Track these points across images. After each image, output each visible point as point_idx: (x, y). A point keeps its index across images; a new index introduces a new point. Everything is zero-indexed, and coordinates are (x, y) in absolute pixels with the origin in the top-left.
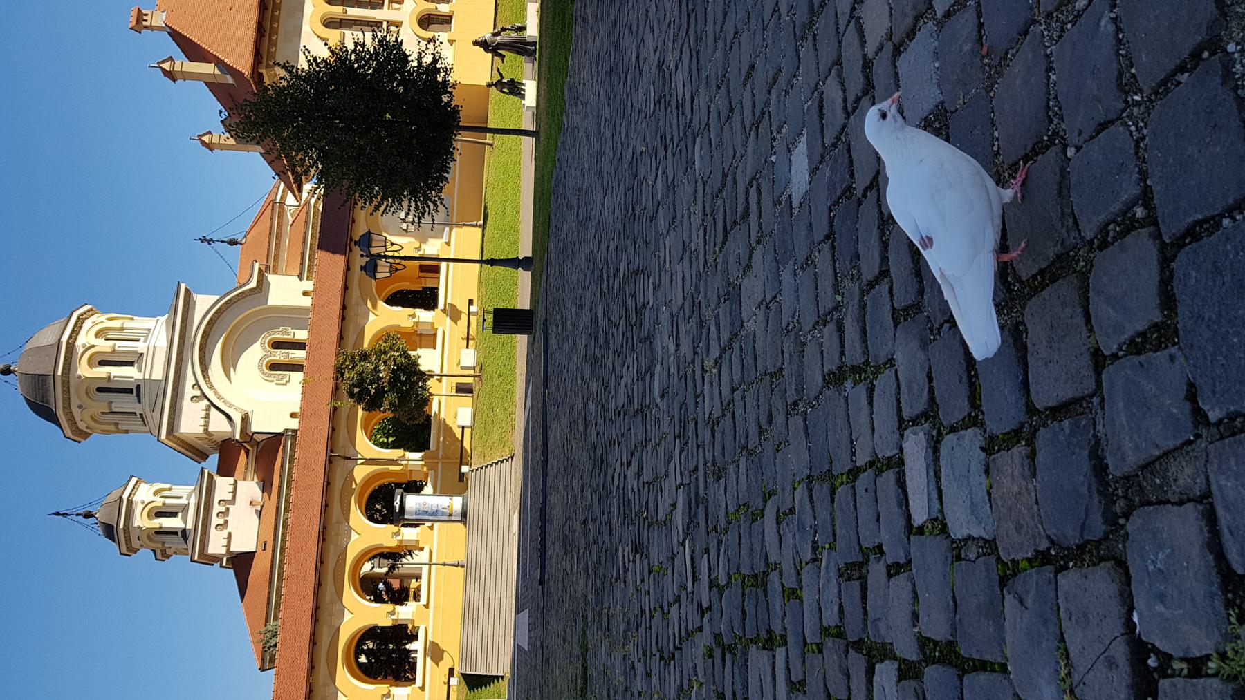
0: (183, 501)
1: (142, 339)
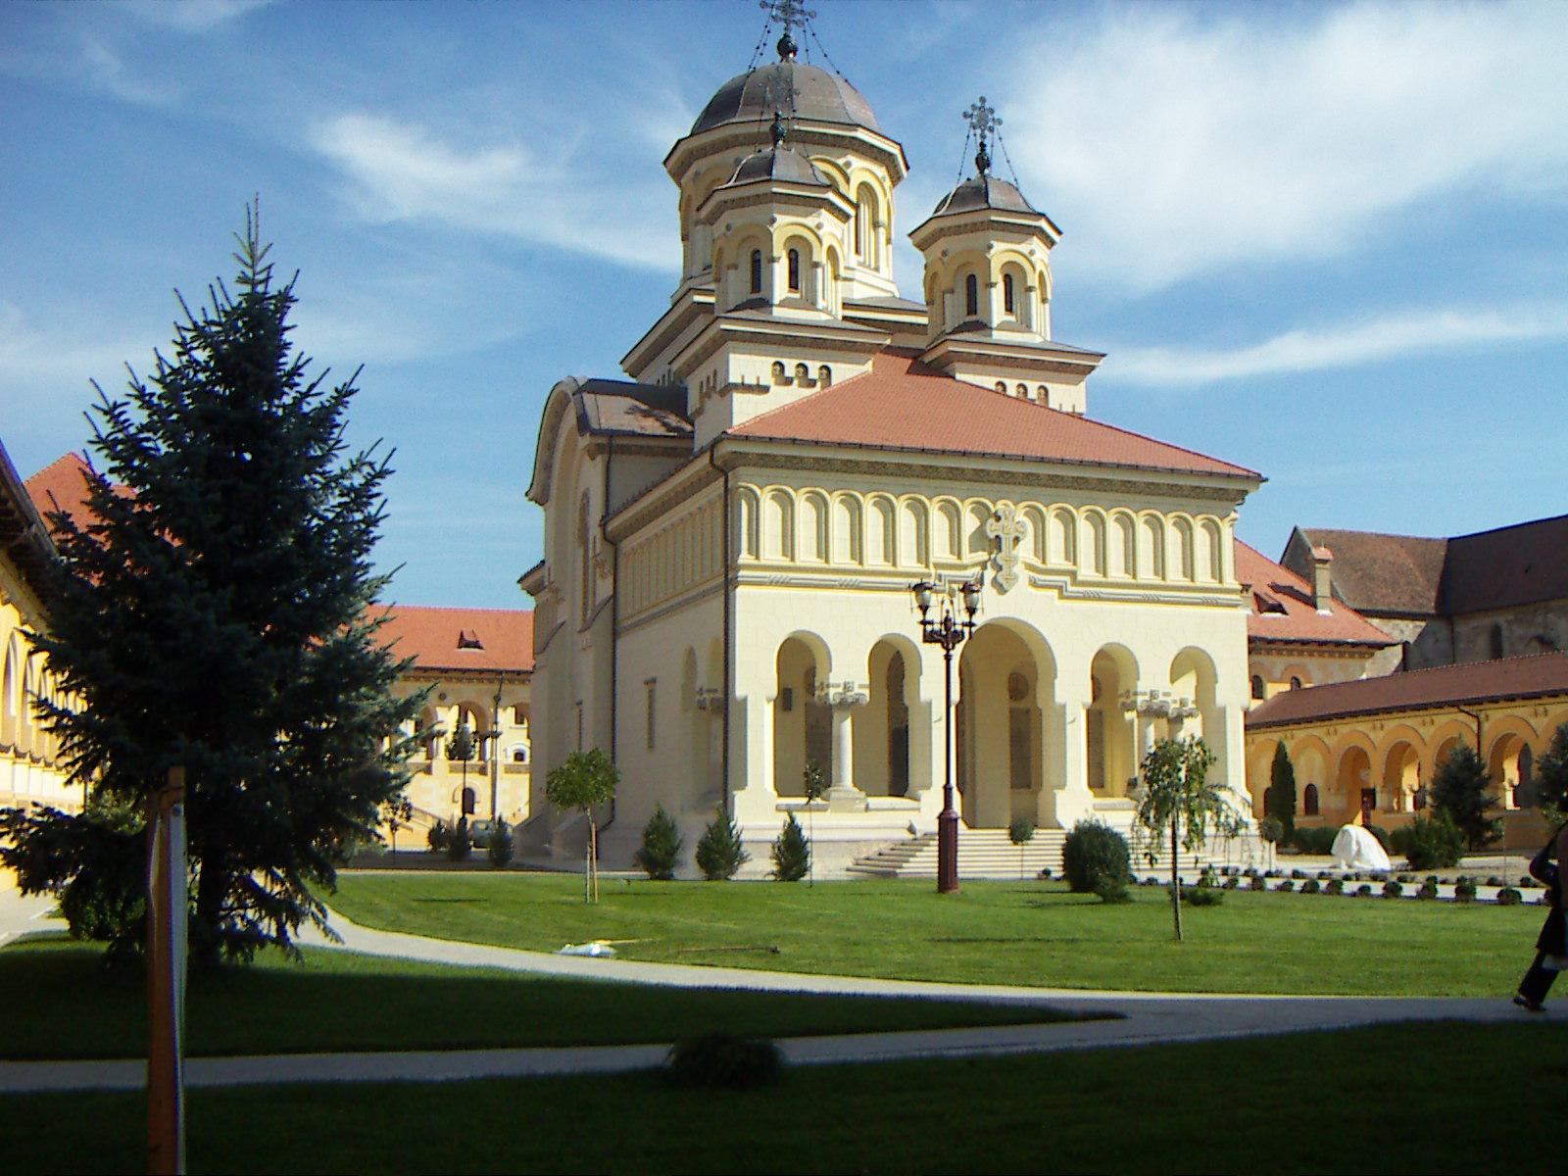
0: (821, 304)
1: (861, 259)
